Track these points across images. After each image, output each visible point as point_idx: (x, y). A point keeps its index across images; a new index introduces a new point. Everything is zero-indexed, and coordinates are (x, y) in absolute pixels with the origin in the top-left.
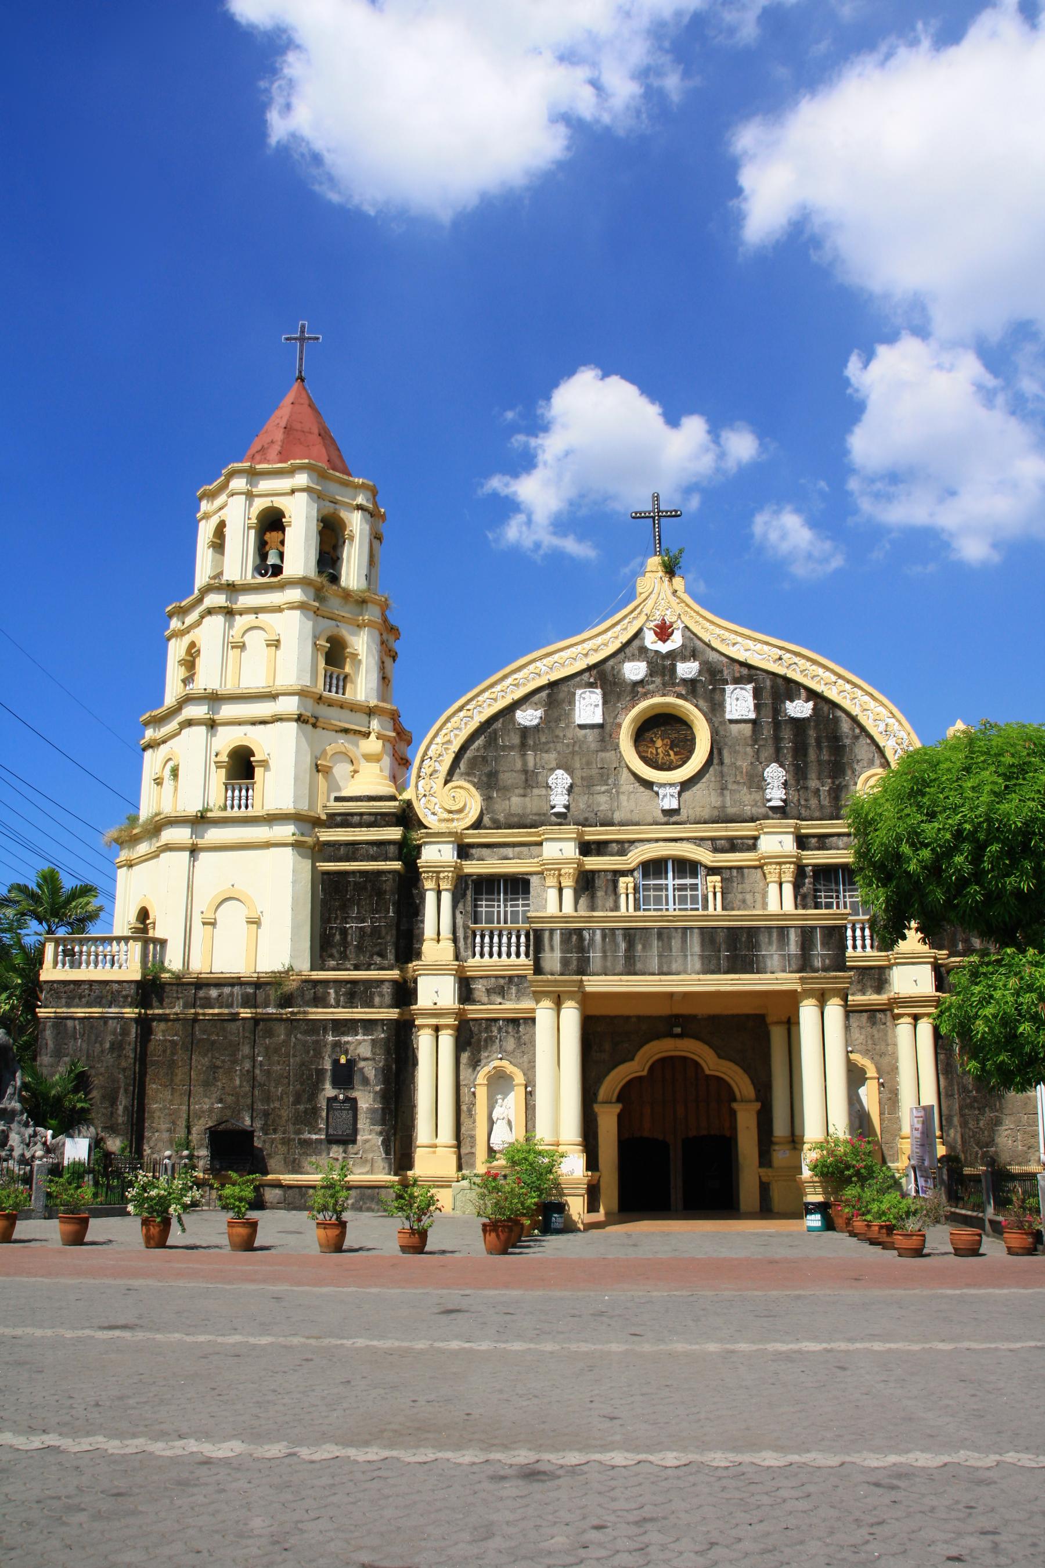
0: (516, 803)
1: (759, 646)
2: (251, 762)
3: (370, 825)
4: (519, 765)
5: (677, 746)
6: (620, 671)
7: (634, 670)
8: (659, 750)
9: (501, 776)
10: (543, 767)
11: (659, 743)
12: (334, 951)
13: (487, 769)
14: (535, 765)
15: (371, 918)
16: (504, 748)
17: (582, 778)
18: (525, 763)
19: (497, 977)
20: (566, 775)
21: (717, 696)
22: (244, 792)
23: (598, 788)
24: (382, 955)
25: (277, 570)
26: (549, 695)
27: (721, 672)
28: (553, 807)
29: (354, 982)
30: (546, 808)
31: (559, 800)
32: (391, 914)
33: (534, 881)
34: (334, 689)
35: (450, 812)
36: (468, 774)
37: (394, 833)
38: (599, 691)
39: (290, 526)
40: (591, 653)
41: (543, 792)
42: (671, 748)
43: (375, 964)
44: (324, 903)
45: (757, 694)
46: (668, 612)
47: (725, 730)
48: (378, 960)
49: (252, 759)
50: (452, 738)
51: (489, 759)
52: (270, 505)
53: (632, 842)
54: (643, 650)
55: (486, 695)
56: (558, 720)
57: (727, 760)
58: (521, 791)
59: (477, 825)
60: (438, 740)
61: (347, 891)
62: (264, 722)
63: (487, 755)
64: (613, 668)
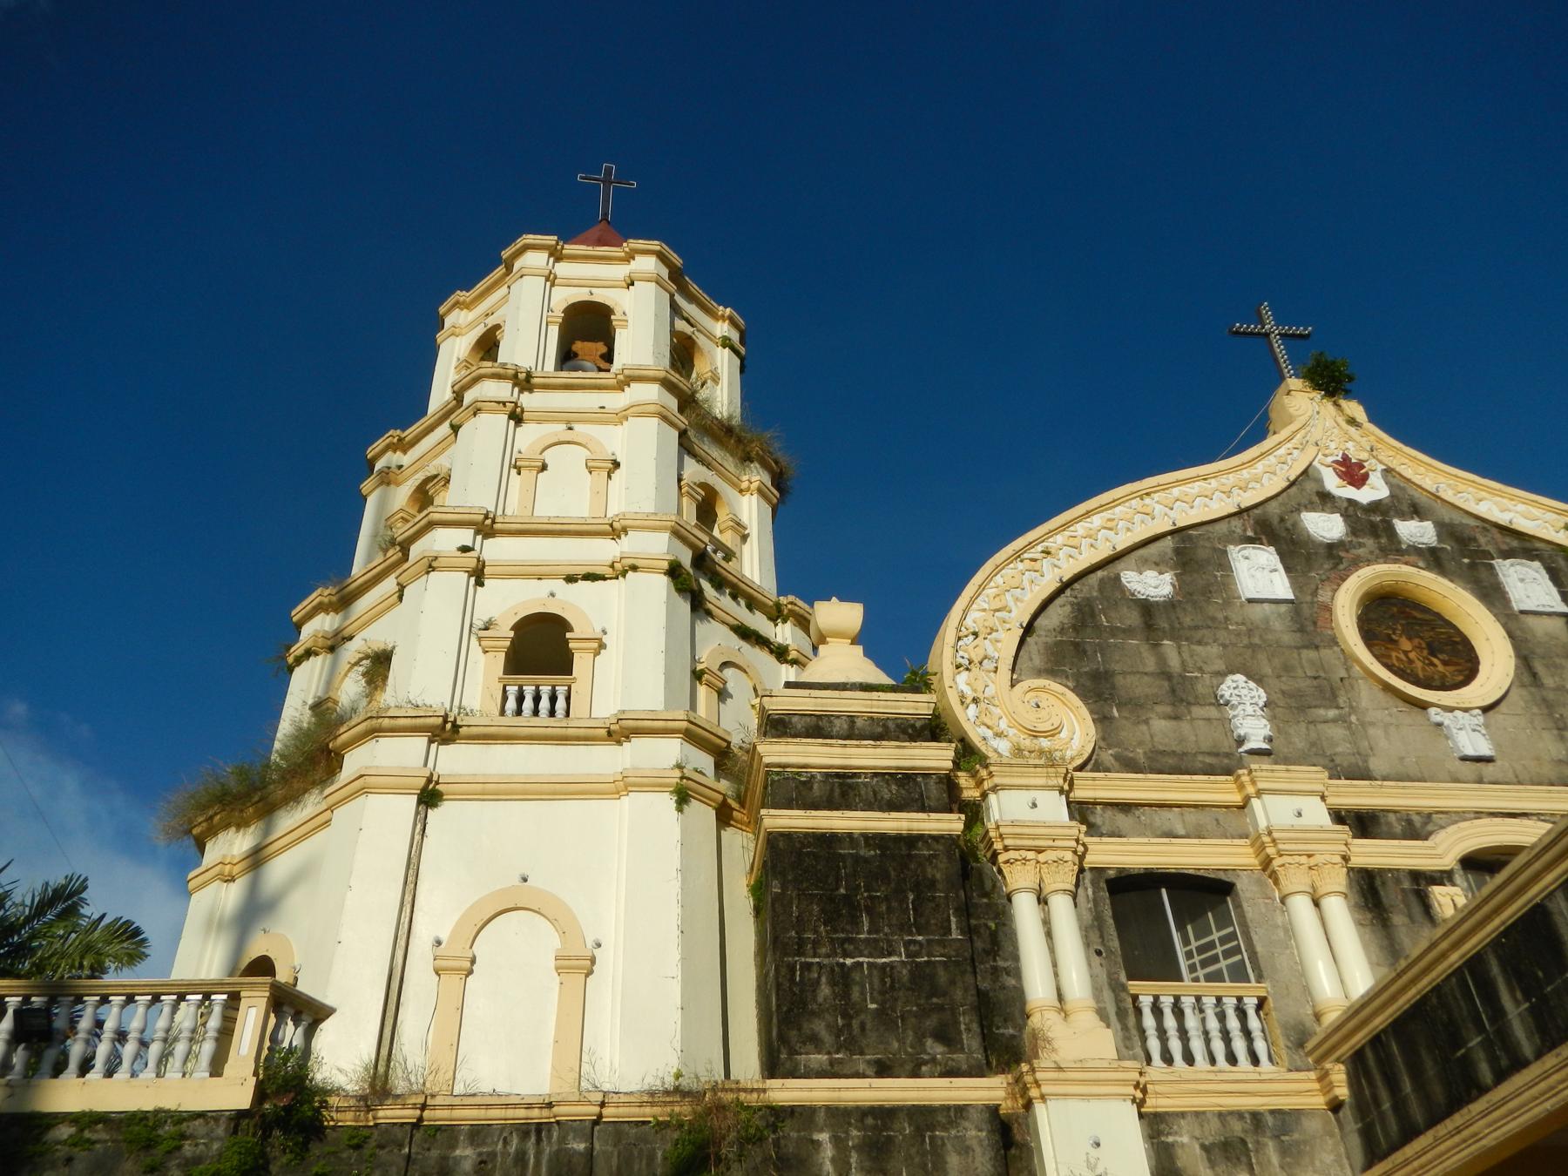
0: (1161, 729)
1: (1521, 507)
2: (566, 642)
4: (1151, 664)
5: (1442, 652)
6: (1295, 525)
7: (1325, 526)
8: (1412, 655)
9: (1119, 680)
10: (1200, 670)
11: (1406, 645)
12: (819, 1027)
14: (1183, 662)
15: (907, 944)
16: (1114, 631)
17: (1283, 692)
18: (1162, 660)
19: (1221, 1116)
20: (1252, 684)
21: (1483, 574)
23: (1322, 712)
24: (946, 1036)
26: (1178, 551)
27: (1475, 540)
28: (1241, 741)
29: (884, 1115)
30: (1227, 745)
31: (1254, 728)
32: (955, 935)
33: (1243, 886)
35: (1035, 734)
36: (1052, 669)
37: (935, 757)
38: (1272, 549)
39: (626, 327)
40: (1236, 491)
41: (1213, 712)
42: (1433, 653)
43: (934, 1060)
45: (1555, 576)
46: (1350, 445)
47: (1522, 630)
48: (936, 1049)
49: (568, 635)
50: (1011, 603)
51: (1088, 648)
52: (587, 298)
53: (1428, 817)
54: (1325, 500)
55: (1059, 539)
56: (1207, 592)
57: (1549, 681)
58: (1168, 709)
59: (1090, 763)
60: (980, 603)
61: (838, 880)
62: (591, 577)
63: (1081, 639)
64: (1282, 520)
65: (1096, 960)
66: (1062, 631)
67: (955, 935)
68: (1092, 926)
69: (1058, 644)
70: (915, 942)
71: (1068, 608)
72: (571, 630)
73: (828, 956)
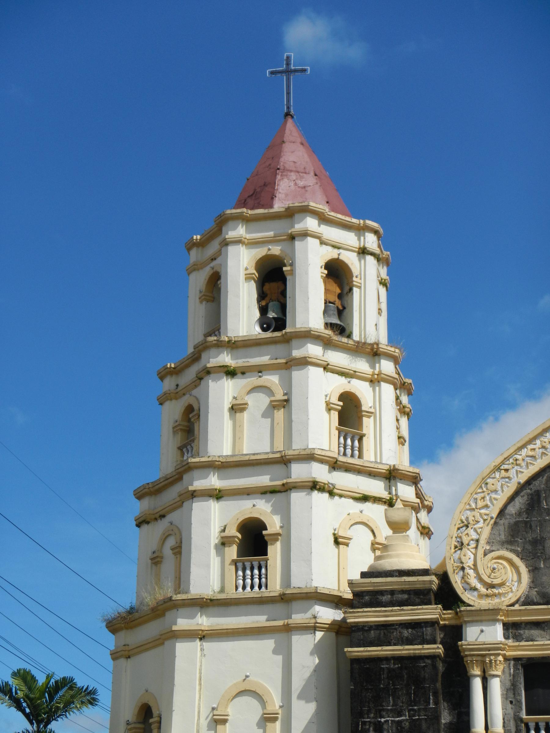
3: (402, 604)
13: (530, 536)
15: (409, 711)
22: (256, 572)
25: (280, 324)
34: (349, 451)
35: (493, 586)
36: (509, 542)
37: (431, 612)
44: (354, 695)
49: (264, 532)
51: (533, 524)
55: (524, 452)
65: (510, 706)
66: (519, 514)
67: (432, 706)
68: (510, 689)
69: (516, 523)
70: (413, 710)
71: (526, 497)
72: (266, 529)
73: (373, 718)
